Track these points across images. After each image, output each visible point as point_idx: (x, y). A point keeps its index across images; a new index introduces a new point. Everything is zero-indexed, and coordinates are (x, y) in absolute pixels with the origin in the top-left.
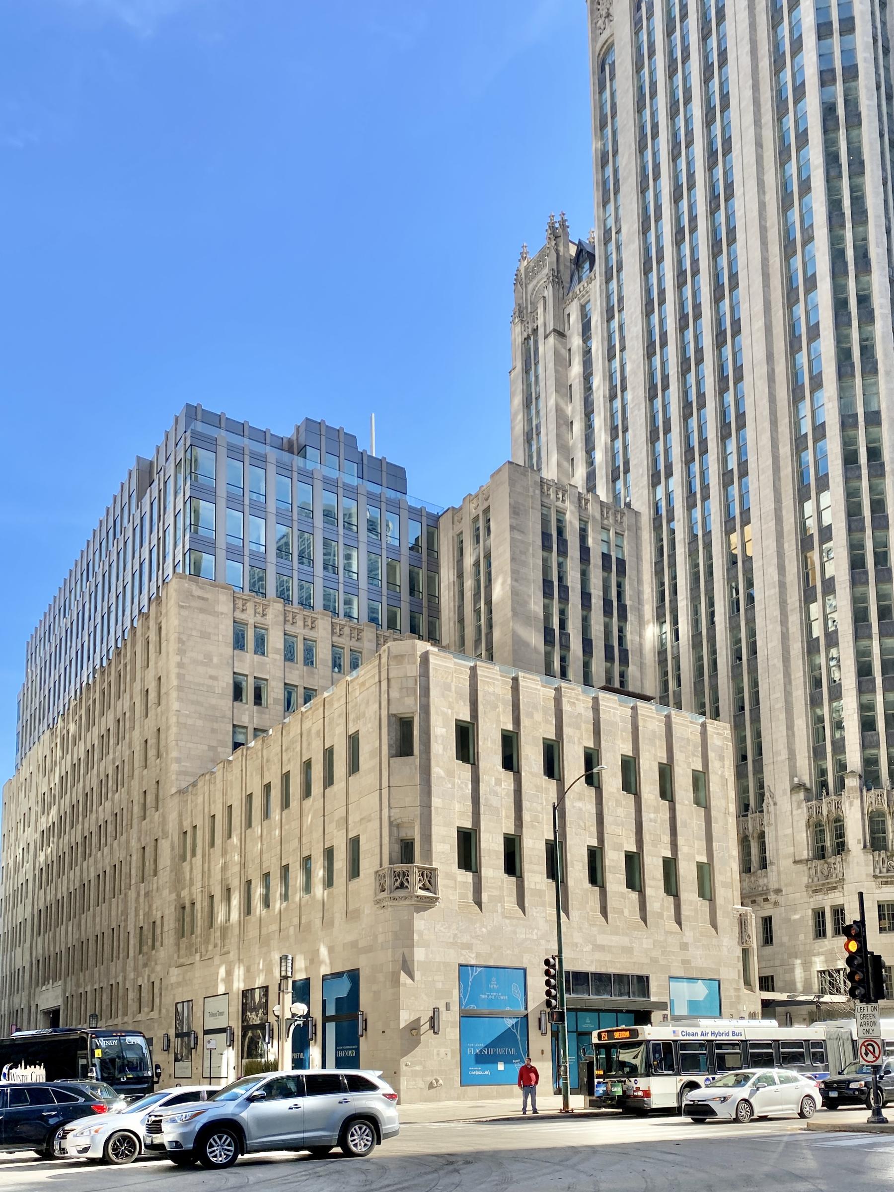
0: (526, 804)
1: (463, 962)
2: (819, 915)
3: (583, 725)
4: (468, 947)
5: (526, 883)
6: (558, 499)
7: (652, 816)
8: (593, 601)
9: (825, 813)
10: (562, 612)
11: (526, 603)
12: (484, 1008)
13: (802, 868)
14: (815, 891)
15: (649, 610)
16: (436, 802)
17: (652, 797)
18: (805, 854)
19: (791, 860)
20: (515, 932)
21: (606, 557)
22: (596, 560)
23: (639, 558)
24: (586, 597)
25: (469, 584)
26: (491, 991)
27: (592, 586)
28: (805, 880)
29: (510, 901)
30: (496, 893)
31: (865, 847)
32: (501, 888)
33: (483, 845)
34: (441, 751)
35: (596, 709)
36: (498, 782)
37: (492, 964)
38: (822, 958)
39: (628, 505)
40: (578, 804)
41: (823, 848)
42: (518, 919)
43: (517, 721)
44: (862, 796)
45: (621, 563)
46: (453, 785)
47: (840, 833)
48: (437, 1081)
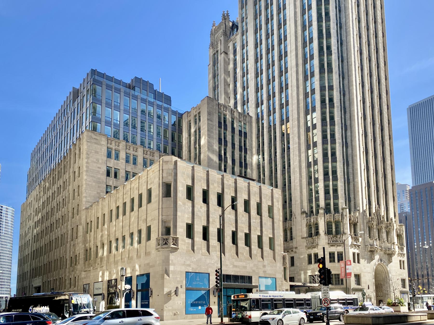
0: (210, 215)
1: (187, 271)
2: (310, 256)
3: (231, 189)
4: (189, 265)
5: (210, 243)
6: (224, 110)
7: (254, 221)
8: (236, 146)
9: (312, 221)
10: (225, 150)
11: (212, 146)
12: (194, 287)
13: (304, 240)
14: (309, 248)
15: (254, 150)
16: (179, 214)
17: (254, 214)
18: (305, 235)
19: (301, 238)
20: (206, 261)
21: (240, 132)
22: (237, 132)
23: (251, 132)
24: (233, 145)
25: (193, 138)
26: (197, 281)
27: (235, 141)
28: (305, 244)
29: (204, 250)
30: (200, 247)
31: (325, 233)
32: (201, 245)
33: (195, 230)
34: (181, 196)
35: (236, 183)
36: (201, 207)
37: (197, 271)
38: (310, 271)
39: (248, 114)
40: (229, 216)
41: (311, 233)
42: (207, 256)
43: (208, 186)
44: (324, 216)
45: (245, 134)
46: (185, 208)
47: (317, 228)
48: (177, 313)
